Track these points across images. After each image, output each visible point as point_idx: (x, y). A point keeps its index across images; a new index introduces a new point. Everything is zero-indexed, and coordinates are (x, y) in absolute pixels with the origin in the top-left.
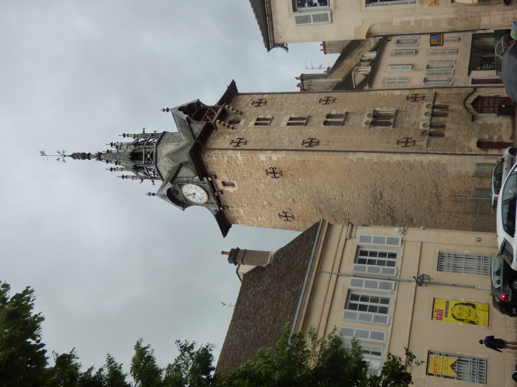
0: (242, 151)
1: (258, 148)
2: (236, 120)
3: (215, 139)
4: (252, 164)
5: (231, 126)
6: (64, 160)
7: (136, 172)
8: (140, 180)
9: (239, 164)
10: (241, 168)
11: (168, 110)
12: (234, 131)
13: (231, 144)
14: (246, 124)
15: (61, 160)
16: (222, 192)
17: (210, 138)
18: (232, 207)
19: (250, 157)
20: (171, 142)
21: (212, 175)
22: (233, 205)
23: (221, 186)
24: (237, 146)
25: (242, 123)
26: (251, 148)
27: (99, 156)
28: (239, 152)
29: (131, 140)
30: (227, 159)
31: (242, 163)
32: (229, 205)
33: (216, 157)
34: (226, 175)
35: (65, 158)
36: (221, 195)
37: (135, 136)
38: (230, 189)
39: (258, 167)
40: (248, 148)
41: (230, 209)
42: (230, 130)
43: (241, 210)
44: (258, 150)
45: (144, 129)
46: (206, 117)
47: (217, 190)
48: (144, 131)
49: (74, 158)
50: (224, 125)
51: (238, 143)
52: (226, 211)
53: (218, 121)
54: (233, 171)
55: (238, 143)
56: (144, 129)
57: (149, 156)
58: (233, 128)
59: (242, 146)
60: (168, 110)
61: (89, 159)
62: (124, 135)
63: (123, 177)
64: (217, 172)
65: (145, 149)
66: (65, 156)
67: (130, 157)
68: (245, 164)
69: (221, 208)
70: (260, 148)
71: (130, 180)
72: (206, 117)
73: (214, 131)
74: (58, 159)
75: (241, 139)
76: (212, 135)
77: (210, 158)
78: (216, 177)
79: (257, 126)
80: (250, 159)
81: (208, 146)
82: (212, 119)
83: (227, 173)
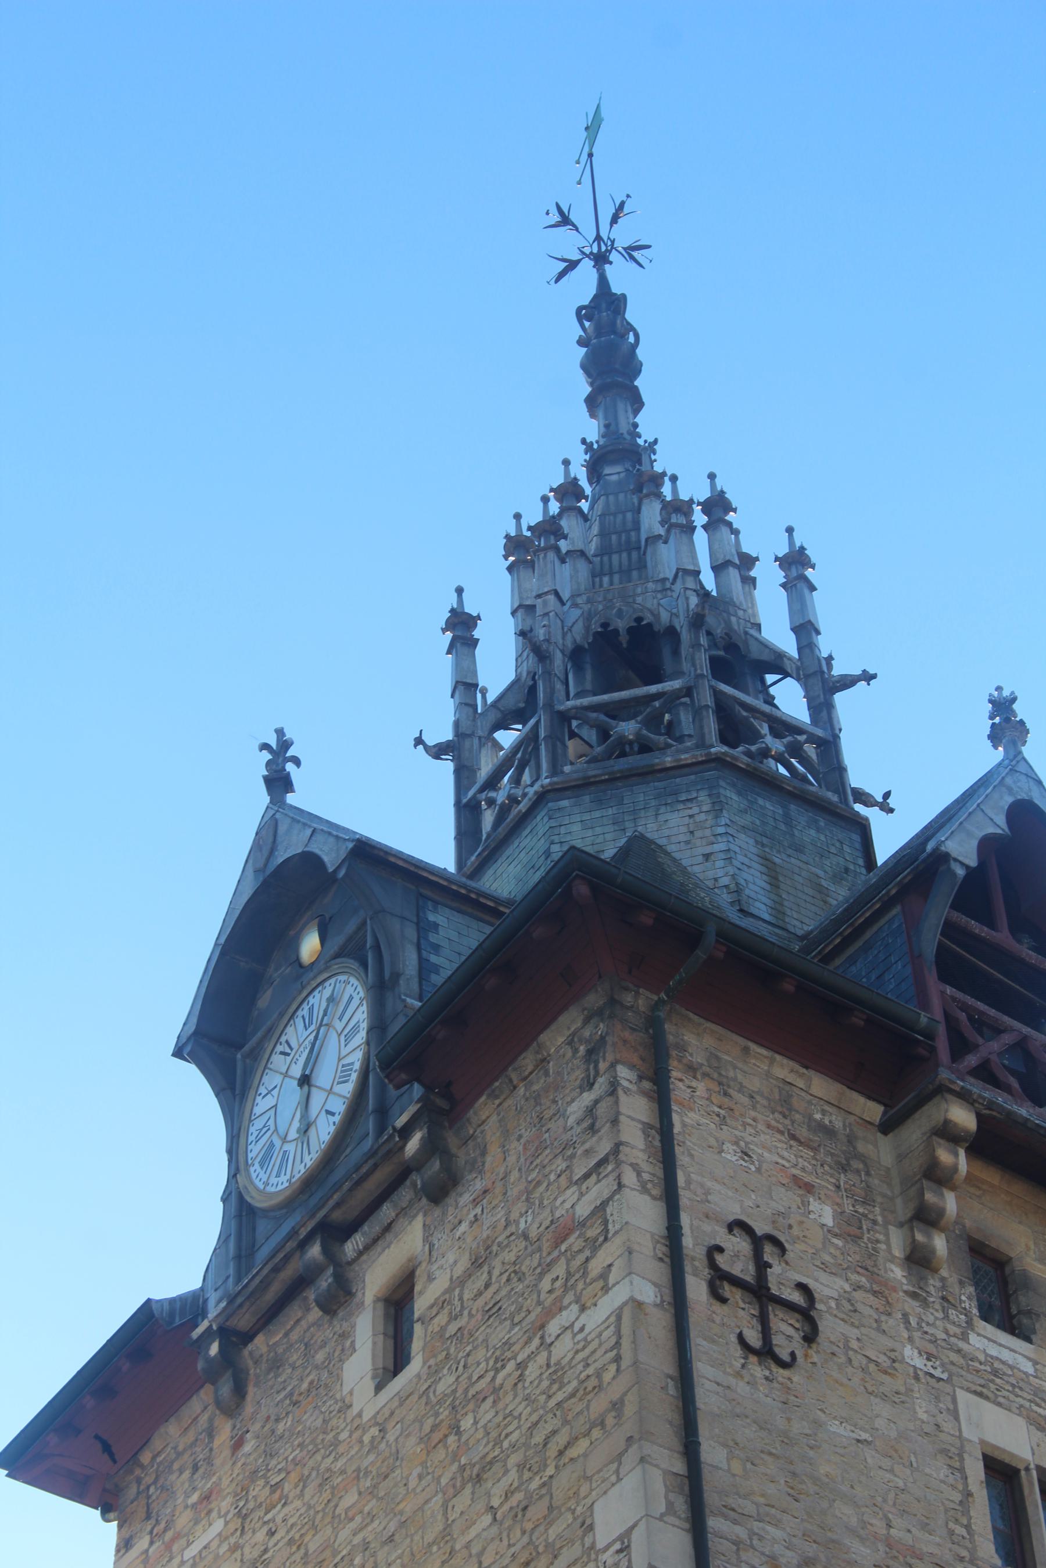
0: (660, 1323)
1: (711, 1453)
2: (1024, 1300)
3: (784, 1102)
4: (561, 1439)
5: (940, 1243)
6: (572, 265)
7: (511, 703)
8: (442, 732)
9: (553, 1328)
10: (521, 1366)
11: (1006, 724)
12: (897, 1273)
13: (738, 1226)
14: (992, 1381)
15: (568, 243)
16: (339, 1299)
17: (784, 1069)
18: (238, 1444)
19: (614, 1393)
20: (766, 860)
21: (447, 1156)
22: (247, 1448)
23: (376, 1277)
24: (719, 1279)
25: (989, 1342)
26: (706, 1398)
27: (620, 458)
28: (646, 1288)
29: (777, 632)
30: (583, 1210)
31: (563, 1349)
32: (249, 1408)
33: (590, 1111)
34: (464, 1264)
35: (587, 264)
36: (316, 1313)
37: (805, 630)
38: (359, 1365)
39: (538, 1511)
40: (703, 1369)
41: (225, 1432)
42: (897, 1243)
43: (218, 1525)
44: (690, 1450)
45: (868, 677)
46: (998, 1031)
47: (350, 1248)
48: (847, 682)
49: (583, 314)
50: (936, 1175)
51: (759, 1292)
52: (200, 1405)
53: (963, 1117)
54: (492, 1312)
55: (759, 1292)
56: (868, 677)
57: (628, 728)
58: (919, 1260)
59: (719, 1327)
60: (1006, 724)
61: (591, 402)
62: (795, 563)
63: (462, 627)
64: (479, 1185)
65: (688, 691)
66: (601, 259)
67: (621, 625)
68: (557, 1374)
69: (214, 1349)
70: (710, 1481)
71: (442, 669)
72: (998, 1031)
73: (874, 1111)
74: (565, 220)
75: (806, 1313)
76: (821, 1086)
77: (579, 1074)
78: (438, 1193)
79: (976, 1471)
80: (599, 1405)
81: (696, 1040)
82: (985, 1073)
83: (477, 1263)
